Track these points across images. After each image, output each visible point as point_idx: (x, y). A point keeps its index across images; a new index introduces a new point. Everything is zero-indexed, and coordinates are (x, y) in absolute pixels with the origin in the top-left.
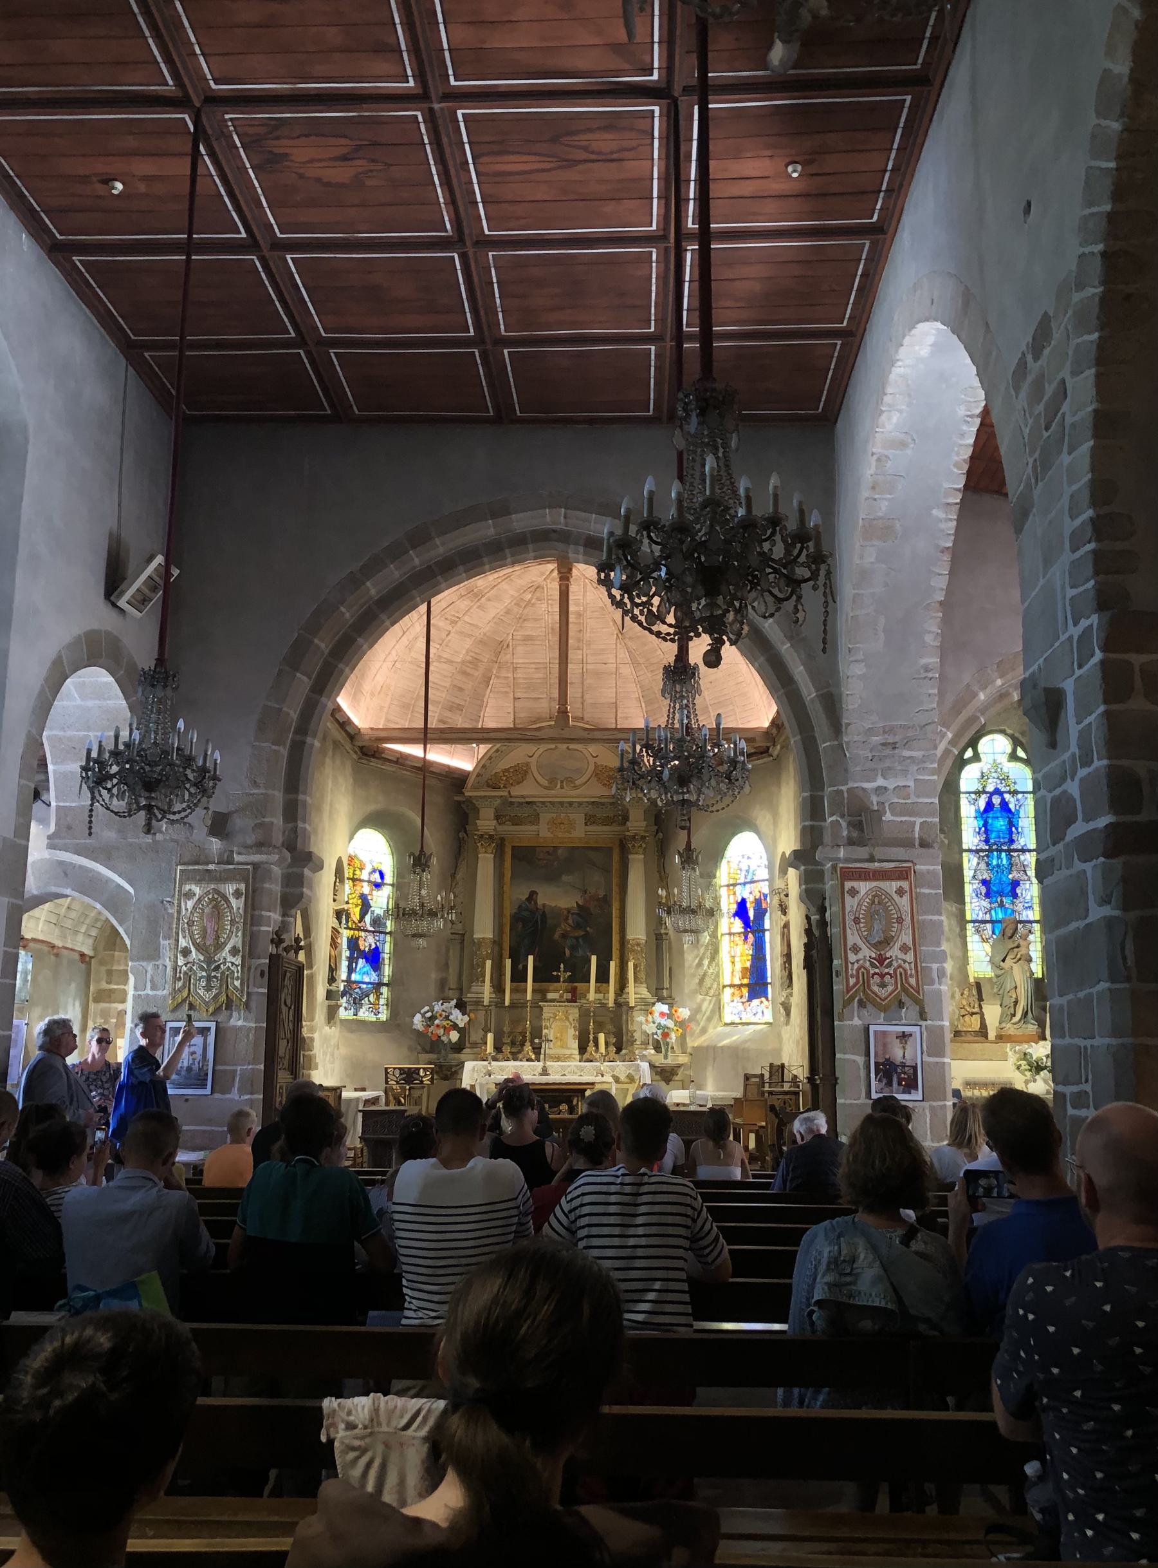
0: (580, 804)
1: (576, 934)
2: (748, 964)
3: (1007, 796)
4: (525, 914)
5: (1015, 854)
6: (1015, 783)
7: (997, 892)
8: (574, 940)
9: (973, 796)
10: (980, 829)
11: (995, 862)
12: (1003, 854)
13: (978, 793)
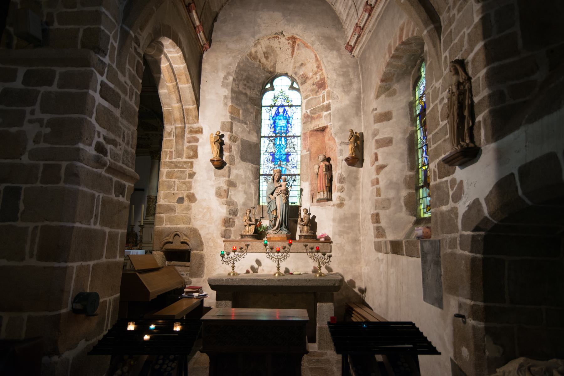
3: (287, 108)
5: (289, 138)
6: (291, 101)
7: (279, 159)
9: (269, 108)
10: (271, 125)
11: (278, 143)
12: (283, 138)
13: (272, 106)
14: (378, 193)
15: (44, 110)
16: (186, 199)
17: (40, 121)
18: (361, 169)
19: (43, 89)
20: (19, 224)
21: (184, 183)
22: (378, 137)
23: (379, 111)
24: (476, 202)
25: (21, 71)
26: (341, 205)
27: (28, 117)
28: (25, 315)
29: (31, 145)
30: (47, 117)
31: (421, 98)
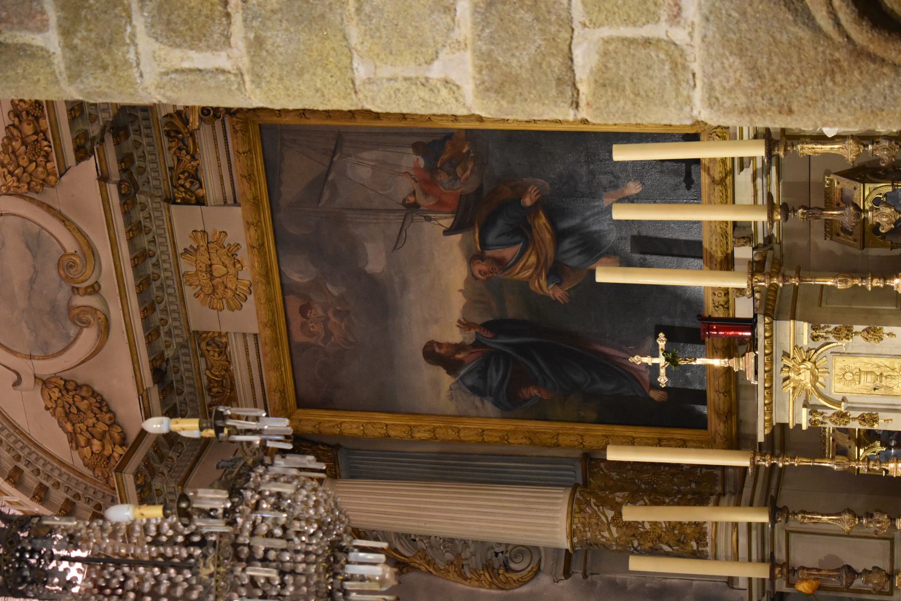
0: (135, 230)
1: (548, 236)
4: (495, 377)
8: (566, 244)
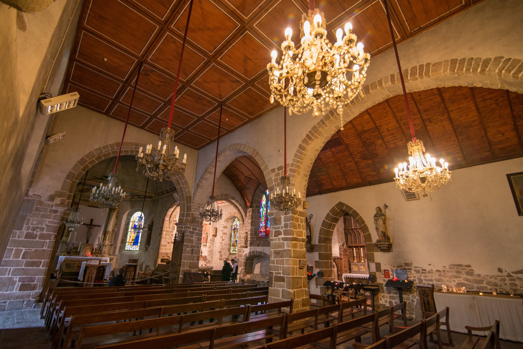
2: (134, 238)
14: (222, 246)
15: (196, 235)
16: (170, 243)
17: (196, 237)
18: (216, 238)
19: (195, 231)
20: (194, 255)
21: (170, 238)
22: (223, 232)
23: (224, 225)
24: (246, 254)
25: (192, 227)
26: (210, 247)
27: (194, 236)
28: (195, 269)
29: (194, 242)
30: (197, 237)
31: (234, 226)
